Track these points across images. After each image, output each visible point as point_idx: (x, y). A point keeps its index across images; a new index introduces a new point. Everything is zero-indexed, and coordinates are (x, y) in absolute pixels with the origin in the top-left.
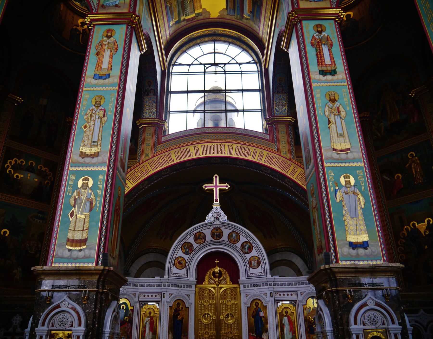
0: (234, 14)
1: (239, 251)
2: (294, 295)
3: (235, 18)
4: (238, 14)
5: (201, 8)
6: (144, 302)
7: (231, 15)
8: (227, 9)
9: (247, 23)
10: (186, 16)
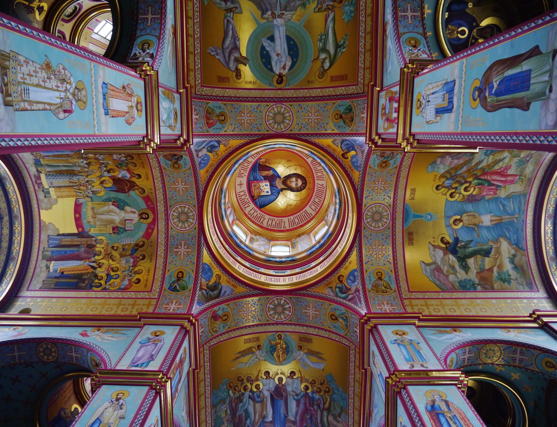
0: (51, 246)
3: (44, 248)
4: (52, 252)
5: (58, 197)
7: (48, 242)
8: (59, 235)
9: (41, 268)
10: (46, 174)
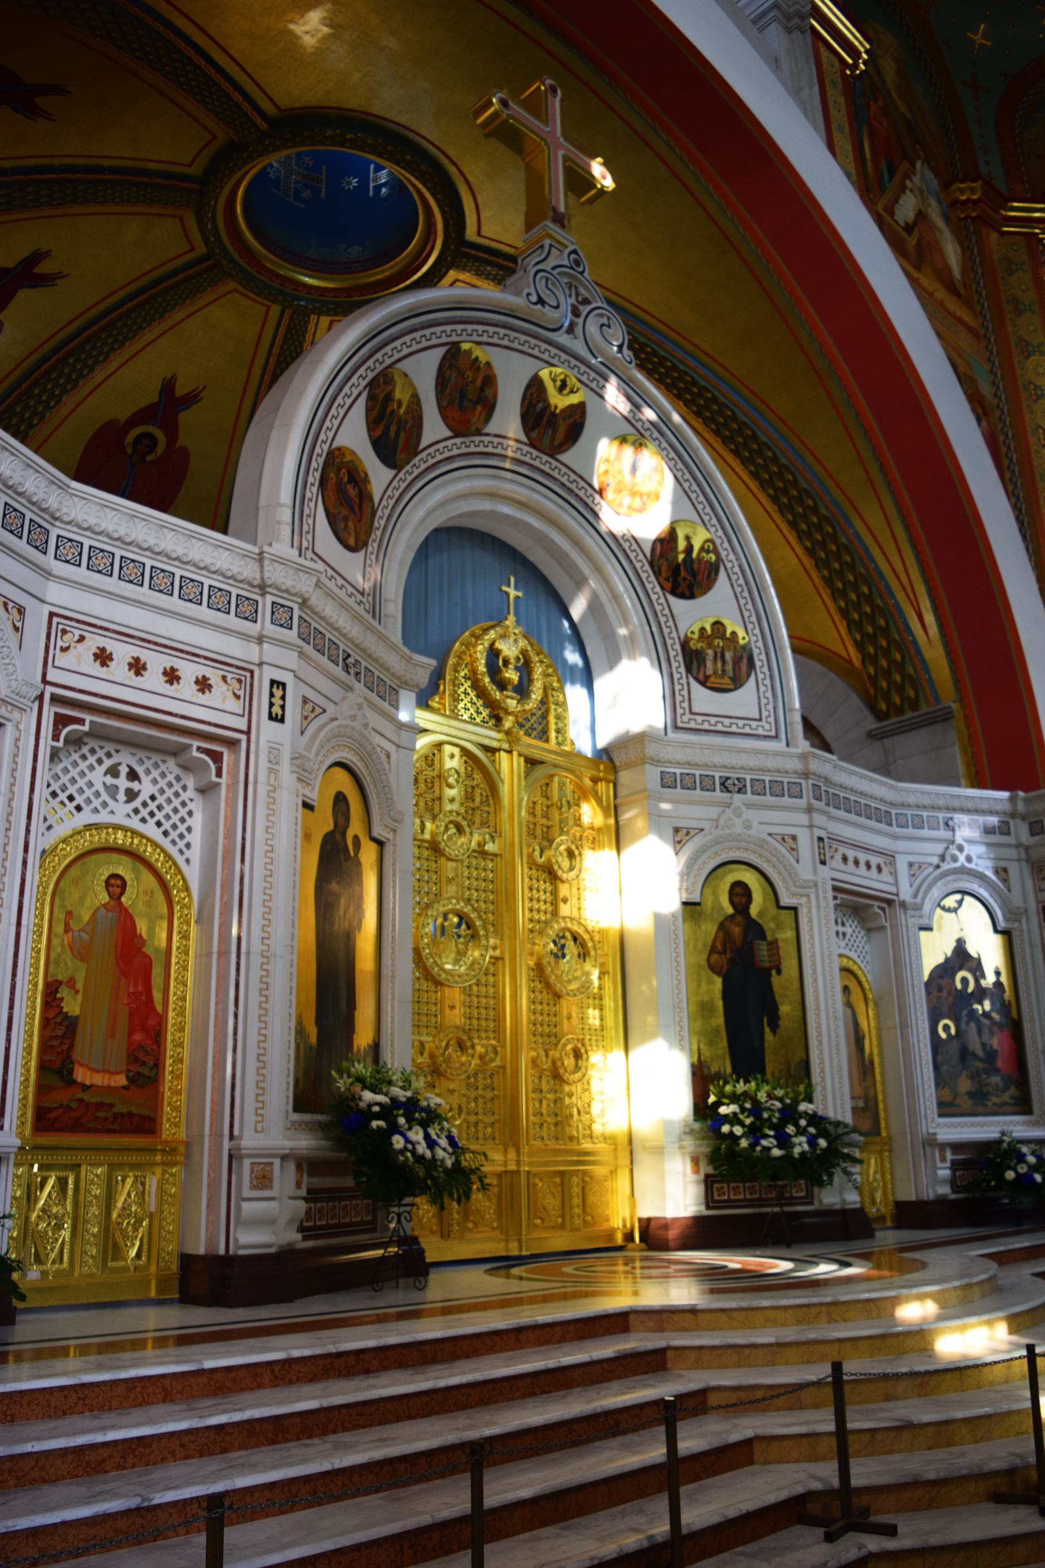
1: (638, 565)
2: (886, 876)
6: (88, 718)
